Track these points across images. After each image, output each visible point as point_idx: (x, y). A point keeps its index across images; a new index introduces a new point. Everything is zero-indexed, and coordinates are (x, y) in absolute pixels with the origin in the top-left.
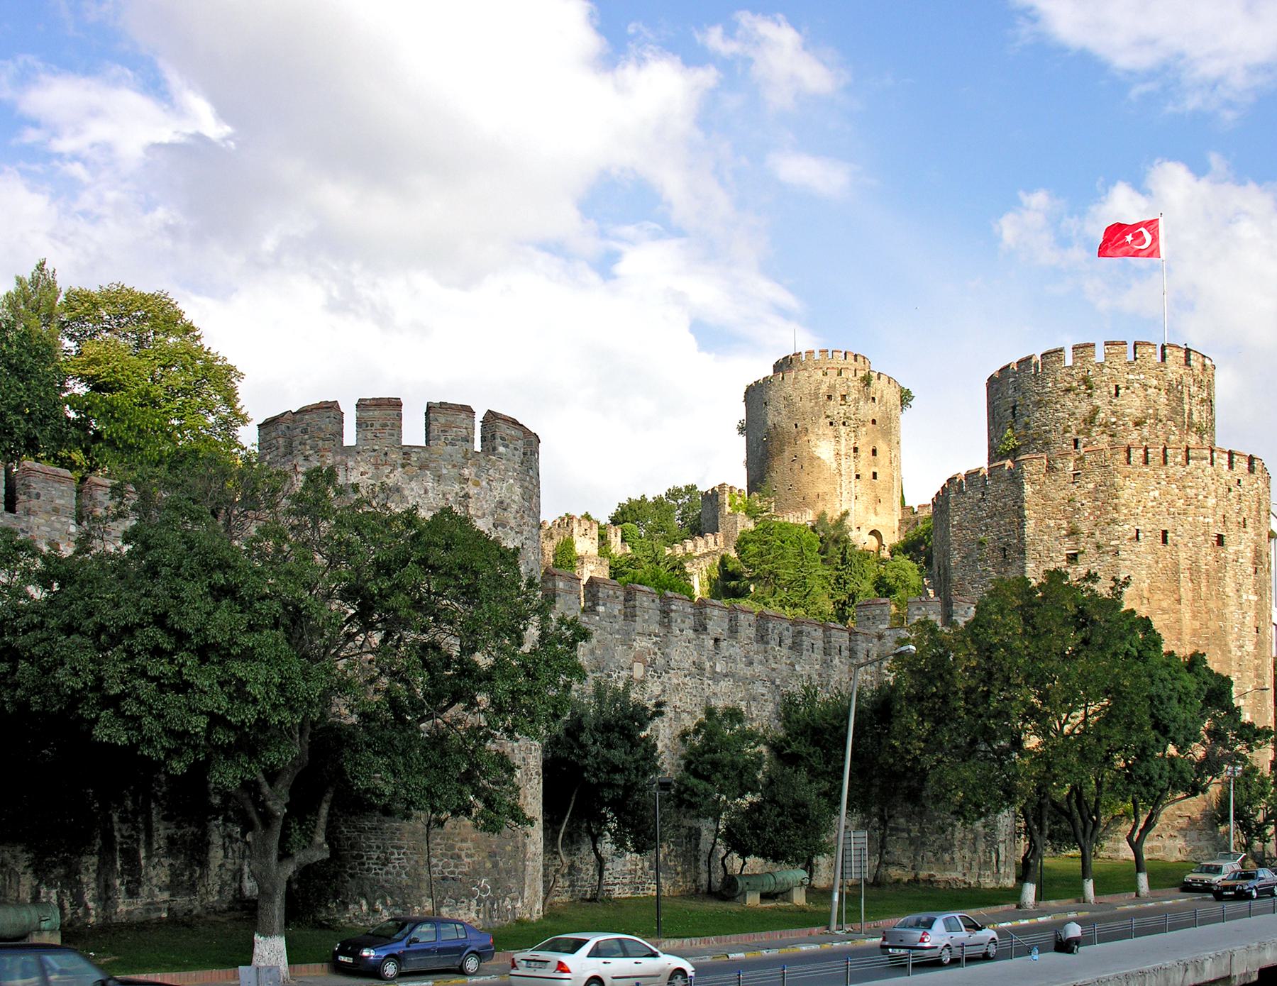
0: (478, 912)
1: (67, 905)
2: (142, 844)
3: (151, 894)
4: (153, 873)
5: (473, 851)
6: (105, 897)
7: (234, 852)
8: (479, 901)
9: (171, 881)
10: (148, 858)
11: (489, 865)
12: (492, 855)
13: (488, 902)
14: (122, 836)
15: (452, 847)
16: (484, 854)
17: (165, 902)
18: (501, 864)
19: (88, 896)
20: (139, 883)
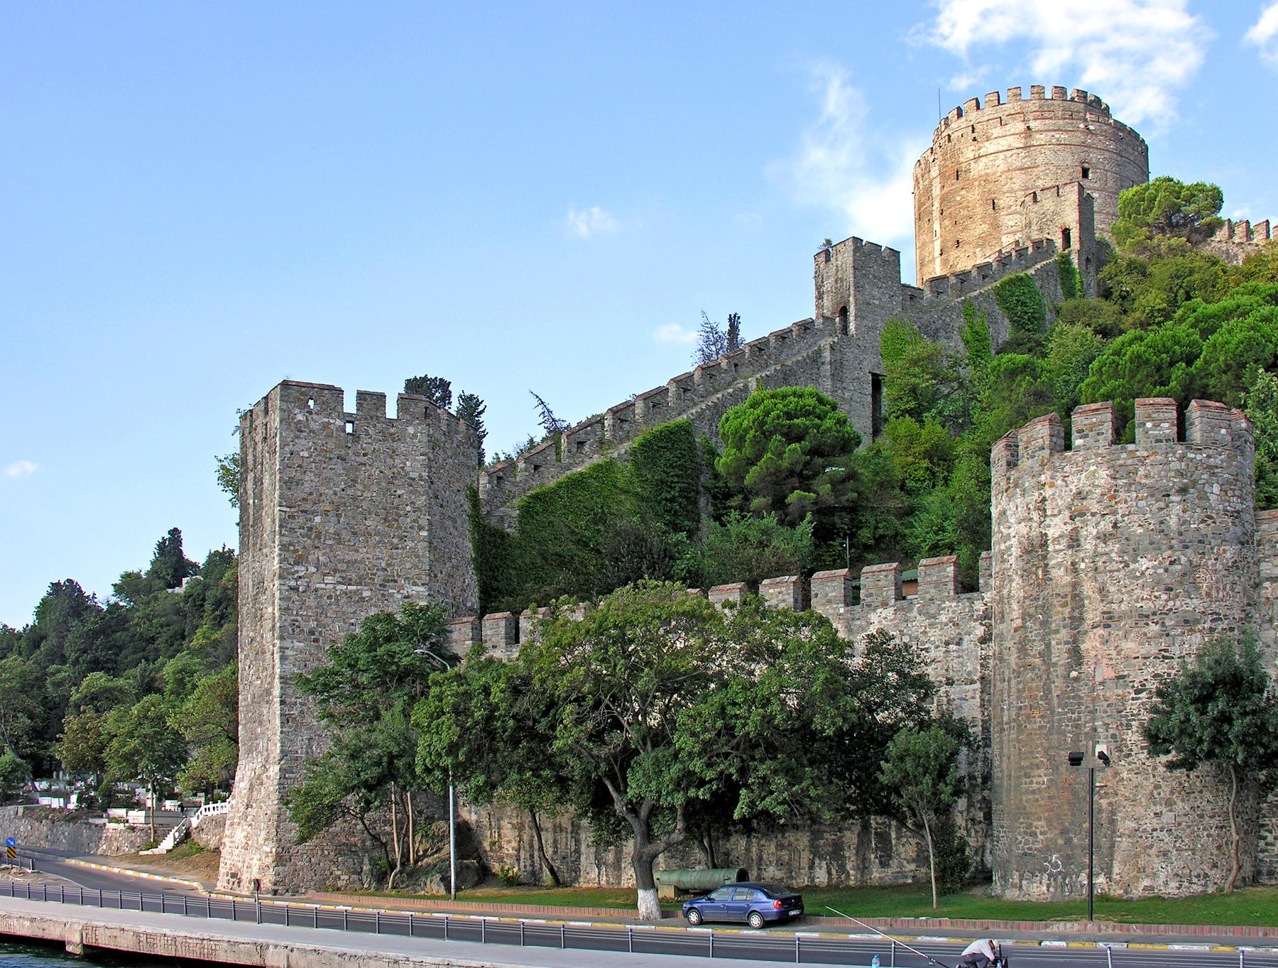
0: (1048, 886)
1: (834, 872)
2: (893, 828)
3: (901, 865)
4: (902, 849)
5: (1046, 829)
6: (864, 867)
7: (977, 832)
8: (1050, 875)
9: (918, 856)
10: (898, 838)
11: (1060, 841)
12: (1064, 832)
13: (1060, 877)
14: (877, 823)
15: (1030, 826)
16: (1057, 832)
17: (911, 871)
18: (1075, 840)
19: (849, 866)
20: (890, 857)
